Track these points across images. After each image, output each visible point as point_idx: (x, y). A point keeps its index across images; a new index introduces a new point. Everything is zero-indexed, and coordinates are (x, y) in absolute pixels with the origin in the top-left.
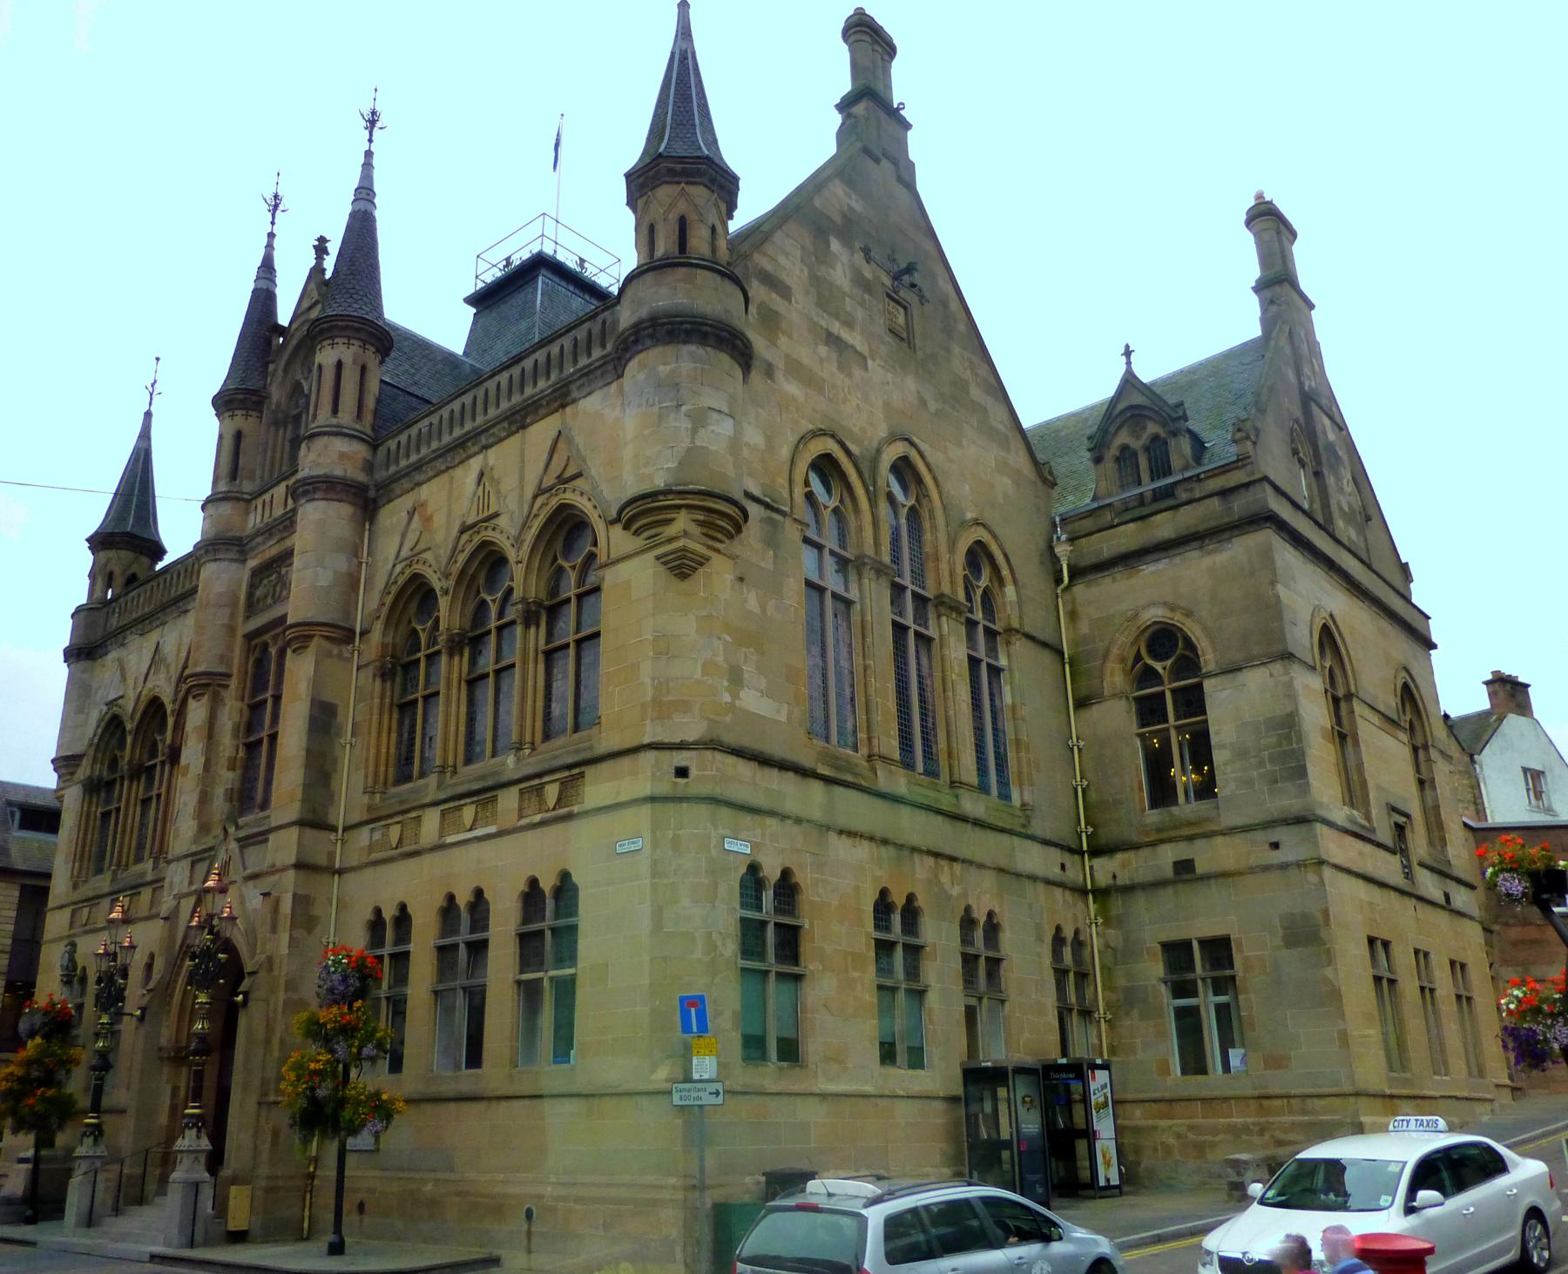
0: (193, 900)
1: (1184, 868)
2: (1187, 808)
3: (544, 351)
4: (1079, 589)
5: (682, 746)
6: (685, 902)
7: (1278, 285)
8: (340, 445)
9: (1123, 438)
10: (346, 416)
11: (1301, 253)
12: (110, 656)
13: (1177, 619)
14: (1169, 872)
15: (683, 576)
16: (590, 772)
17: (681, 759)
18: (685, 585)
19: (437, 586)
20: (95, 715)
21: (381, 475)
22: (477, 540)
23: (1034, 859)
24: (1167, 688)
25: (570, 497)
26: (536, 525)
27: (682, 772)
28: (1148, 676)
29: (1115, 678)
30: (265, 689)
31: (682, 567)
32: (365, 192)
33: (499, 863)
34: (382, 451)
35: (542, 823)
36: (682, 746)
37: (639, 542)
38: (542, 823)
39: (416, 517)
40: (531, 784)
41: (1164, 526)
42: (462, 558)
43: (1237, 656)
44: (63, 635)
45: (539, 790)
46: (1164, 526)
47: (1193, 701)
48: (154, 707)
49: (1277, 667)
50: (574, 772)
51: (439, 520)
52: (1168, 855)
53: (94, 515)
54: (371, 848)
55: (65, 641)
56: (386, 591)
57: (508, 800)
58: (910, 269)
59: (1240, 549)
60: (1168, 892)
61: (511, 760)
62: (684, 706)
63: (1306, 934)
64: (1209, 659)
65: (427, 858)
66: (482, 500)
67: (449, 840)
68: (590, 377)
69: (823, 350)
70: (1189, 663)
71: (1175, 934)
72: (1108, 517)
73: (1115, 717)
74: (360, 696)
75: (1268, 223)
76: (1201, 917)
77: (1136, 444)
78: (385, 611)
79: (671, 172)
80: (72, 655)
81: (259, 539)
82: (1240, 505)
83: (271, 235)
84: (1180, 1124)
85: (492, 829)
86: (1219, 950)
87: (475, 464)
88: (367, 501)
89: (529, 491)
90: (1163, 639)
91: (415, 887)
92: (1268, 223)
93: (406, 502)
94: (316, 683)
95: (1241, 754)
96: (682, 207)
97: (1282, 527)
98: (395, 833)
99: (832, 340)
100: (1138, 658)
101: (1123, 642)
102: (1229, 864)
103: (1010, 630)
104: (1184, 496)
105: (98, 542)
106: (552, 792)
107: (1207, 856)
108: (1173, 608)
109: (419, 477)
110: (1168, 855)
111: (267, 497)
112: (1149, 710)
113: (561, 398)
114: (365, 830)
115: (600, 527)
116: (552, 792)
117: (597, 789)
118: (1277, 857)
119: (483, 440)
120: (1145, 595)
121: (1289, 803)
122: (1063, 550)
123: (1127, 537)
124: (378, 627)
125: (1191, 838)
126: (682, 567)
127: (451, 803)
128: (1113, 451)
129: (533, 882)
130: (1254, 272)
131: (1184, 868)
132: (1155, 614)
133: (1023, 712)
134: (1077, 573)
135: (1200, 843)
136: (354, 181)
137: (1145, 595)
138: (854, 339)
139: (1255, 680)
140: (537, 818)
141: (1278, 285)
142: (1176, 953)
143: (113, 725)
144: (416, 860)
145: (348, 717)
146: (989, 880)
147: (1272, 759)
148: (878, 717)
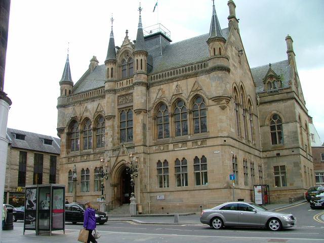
0: (115, 158)
1: (278, 155)
2: (278, 145)
3: (191, 66)
4: (261, 106)
5: (225, 137)
6: (226, 160)
7: (290, 52)
8: (143, 76)
9: (269, 80)
10: (143, 70)
11: (294, 44)
12: (70, 108)
13: (278, 113)
14: (276, 155)
15: (223, 110)
16: (207, 140)
17: (225, 139)
18: (223, 111)
19: (168, 105)
20: (68, 120)
21: (151, 82)
22: (177, 97)
23: (257, 153)
24: (276, 125)
25: (198, 93)
26: (191, 97)
27: (225, 141)
28: (272, 122)
29: (267, 122)
30: (124, 118)
31: (223, 108)
33: (189, 154)
34: (150, 77)
35: (198, 148)
36: (225, 137)
37: (216, 103)
38: (198, 148)
39: (160, 91)
40: (195, 141)
41: (276, 97)
42: (173, 100)
43: (288, 120)
44: (56, 103)
45: (196, 142)
46: (276, 97)
47: (280, 127)
48: (87, 119)
49: (295, 123)
50: (204, 140)
51: (167, 92)
52: (275, 152)
53: (59, 77)
54: (156, 150)
55: (57, 105)
56: (154, 104)
57: (190, 144)
58: (241, 51)
59: (289, 103)
60: (275, 158)
61: (189, 137)
62: (225, 131)
63: (297, 165)
64: (283, 121)
66: (178, 91)
68: (203, 73)
69: (233, 67)
70: (280, 121)
71: (276, 165)
72: (266, 94)
73: (268, 129)
74: (149, 121)
75: (289, 39)
76: (280, 162)
77: (272, 82)
78: (154, 108)
79: (218, 40)
80: (59, 107)
82: (290, 95)
84: (276, 194)
85: (186, 148)
86: (283, 167)
87: (175, 83)
88: (148, 86)
89: (190, 91)
90: (275, 116)
91: (170, 157)
92: (289, 39)
93: (158, 87)
94: (143, 120)
95: (288, 136)
96: (220, 46)
97: (297, 101)
98: (162, 148)
99: (234, 66)
100: (271, 119)
101: (269, 117)
102: (285, 154)
103: (253, 114)
104: (280, 92)
105: (62, 83)
106: (199, 143)
107: (282, 153)
108: (278, 111)
109: (161, 83)
110: (275, 152)
111: (121, 82)
112: (273, 128)
113: (196, 75)
114: (155, 147)
115: (207, 100)
116: (199, 143)
118: (293, 153)
120: (273, 108)
121: (296, 145)
122: (258, 99)
123: (270, 98)
124: (153, 110)
125: (279, 150)
126: (223, 108)
127: (176, 143)
128: (267, 82)
130: (286, 50)
131: (278, 155)
132: (275, 112)
133: (255, 128)
134: (261, 103)
135: (281, 151)
136: (138, 22)
137: (273, 108)
138: (236, 65)
139: (291, 124)
141: (290, 52)
142: (276, 168)
143: (73, 122)
144: (168, 153)
145: (147, 127)
146: (252, 156)
147: (293, 137)
148: (242, 130)
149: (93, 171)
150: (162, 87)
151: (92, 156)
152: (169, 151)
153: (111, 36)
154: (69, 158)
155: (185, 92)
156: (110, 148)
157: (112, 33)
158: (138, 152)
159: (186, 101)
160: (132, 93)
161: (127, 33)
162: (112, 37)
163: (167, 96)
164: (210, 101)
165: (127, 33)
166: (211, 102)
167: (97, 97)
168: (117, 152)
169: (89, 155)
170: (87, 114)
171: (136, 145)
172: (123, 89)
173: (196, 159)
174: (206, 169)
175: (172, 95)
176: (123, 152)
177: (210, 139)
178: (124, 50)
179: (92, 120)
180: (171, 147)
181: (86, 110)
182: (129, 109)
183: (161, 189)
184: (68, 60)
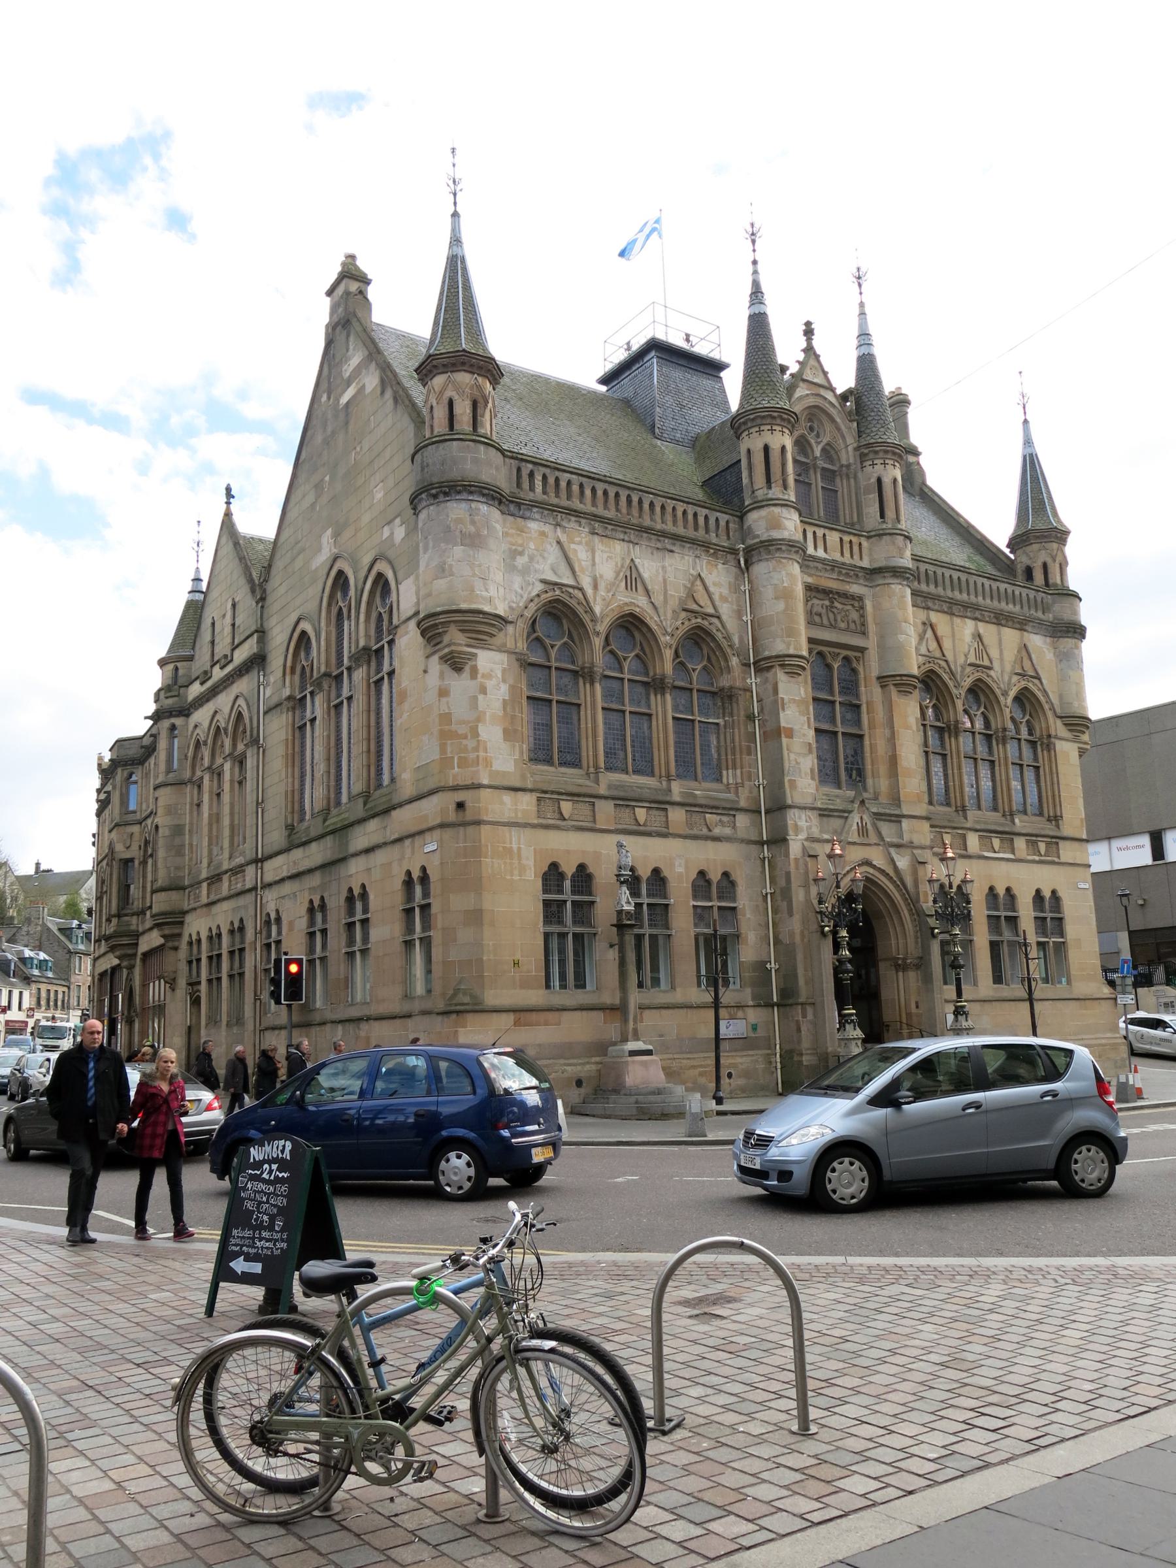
16: (1062, 844)
25: (1030, 685)
32: (864, 337)
35: (1033, 862)
65: (974, 861)
67: (986, 854)
81: (820, 566)
83: (755, 262)
85: (1011, 856)
106: (1042, 847)
113: (1021, 625)
115: (1050, 714)
117: (1067, 852)
119: (977, 614)
129: (1038, 891)
140: (1037, 858)
149: (687, 886)
150: (935, 617)
151: (677, 816)
152: (969, 857)
153: (752, 304)
154: (546, 795)
155: (996, 665)
156: (808, 801)
157: (756, 294)
158: (916, 842)
159: (1002, 699)
160: (860, 599)
161: (809, 332)
162: (757, 309)
163: (949, 656)
164: (1059, 722)
165: (809, 332)
166: (1057, 727)
167: (693, 542)
168: (836, 823)
169: (661, 804)
170: (640, 603)
171: (905, 813)
172: (833, 566)
173: (1038, 896)
174: (1062, 935)
175: (961, 660)
176: (863, 831)
177: (1068, 843)
178: (812, 401)
179: (664, 639)
180: (973, 841)
181: (632, 579)
182: (852, 658)
183: (1004, 991)
184: (456, 241)
